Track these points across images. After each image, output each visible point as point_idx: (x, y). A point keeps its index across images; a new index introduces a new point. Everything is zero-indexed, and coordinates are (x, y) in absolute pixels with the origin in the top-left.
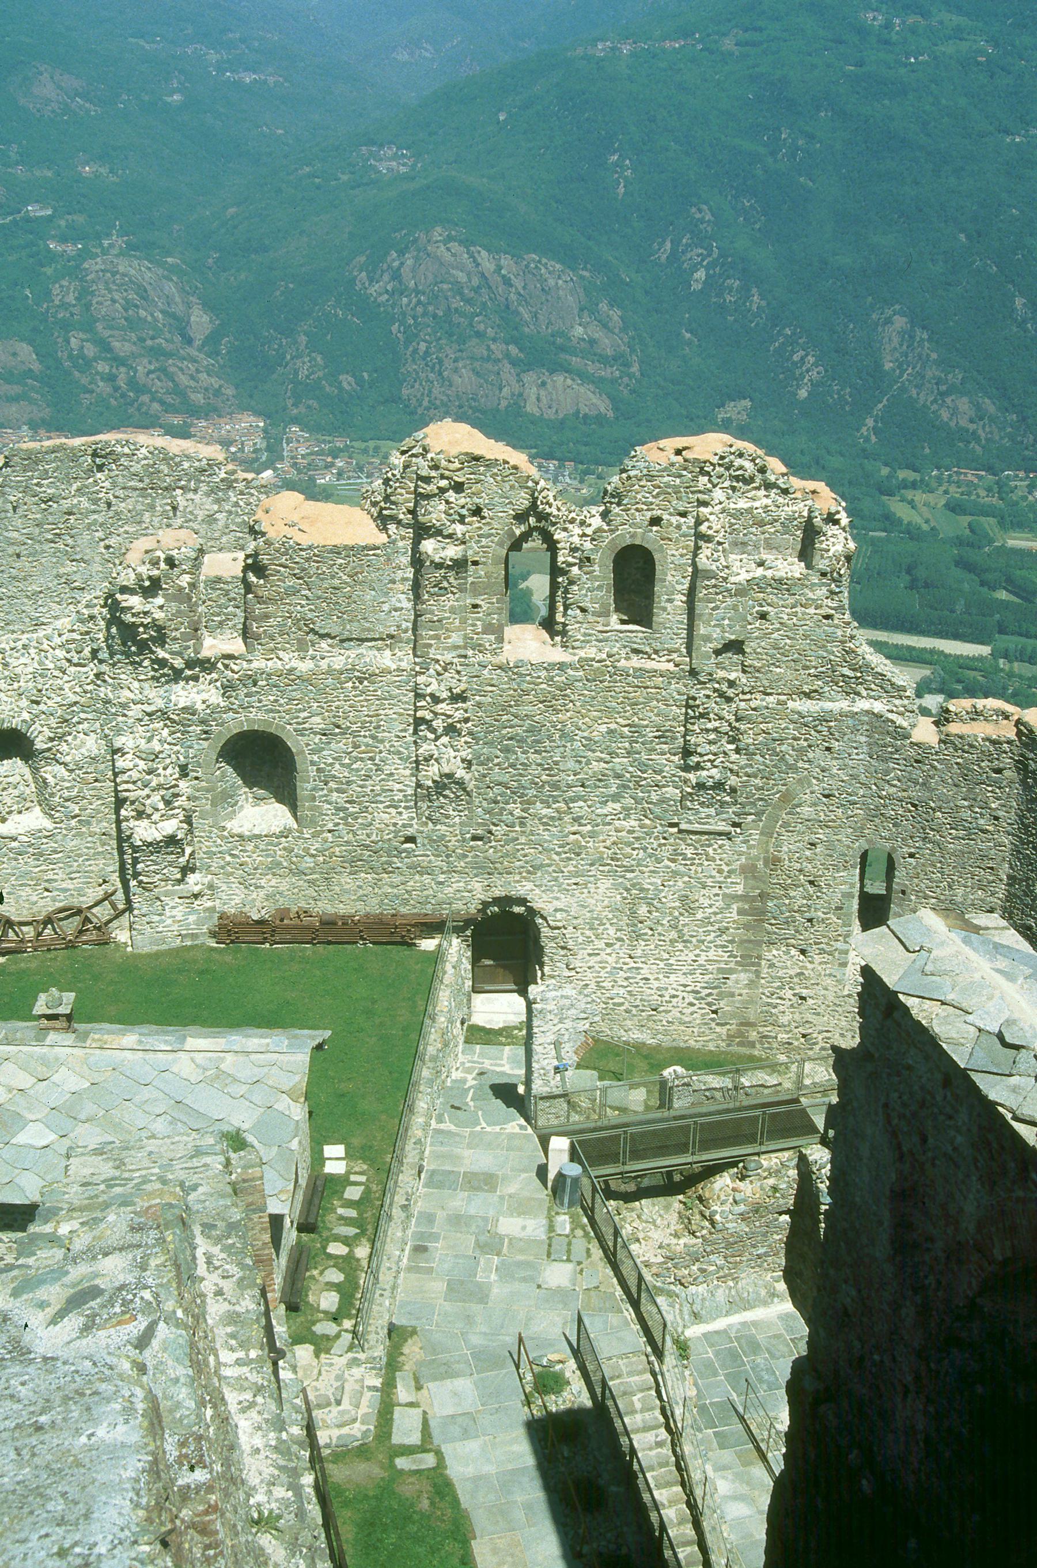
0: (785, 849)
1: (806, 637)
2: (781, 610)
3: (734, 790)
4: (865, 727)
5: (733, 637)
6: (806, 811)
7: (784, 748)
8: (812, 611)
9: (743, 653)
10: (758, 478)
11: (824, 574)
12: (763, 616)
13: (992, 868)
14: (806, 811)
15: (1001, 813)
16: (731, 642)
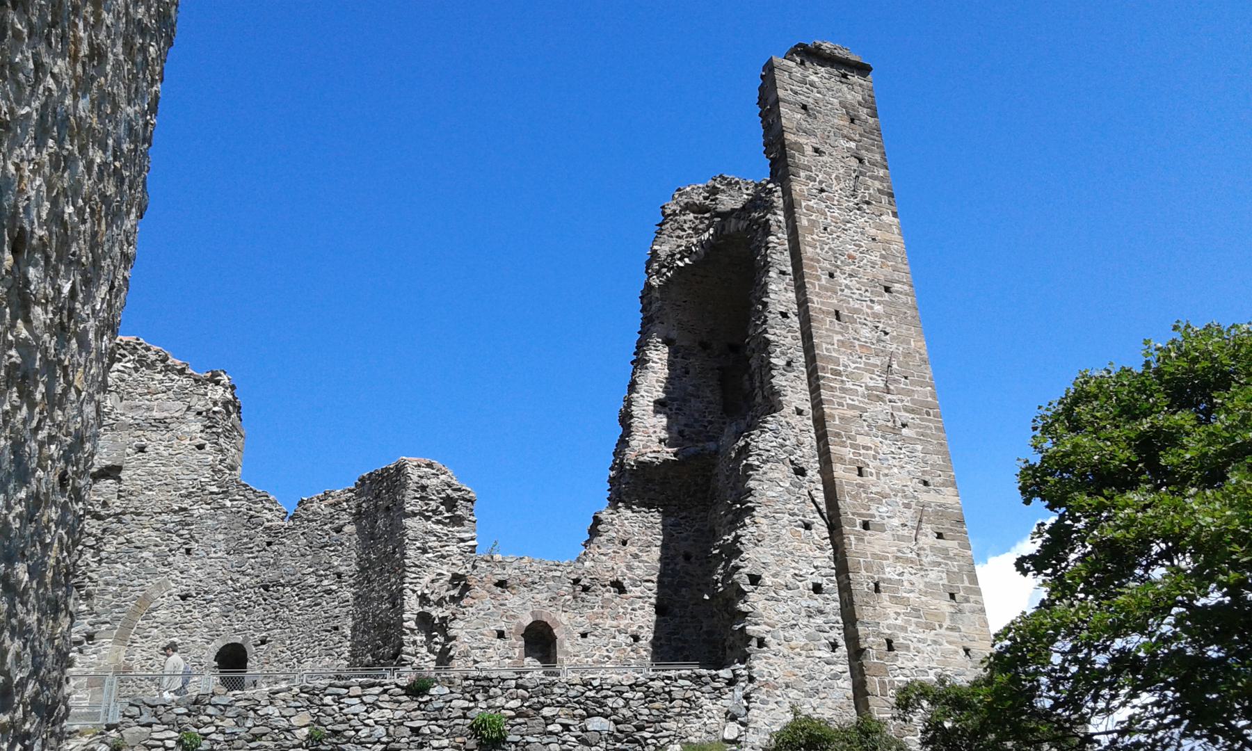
0: (137, 656)
1: (179, 463)
2: (156, 441)
3: (89, 596)
4: (224, 525)
5: (109, 463)
6: (162, 614)
7: (145, 554)
8: (187, 442)
9: (119, 480)
10: (160, 366)
11: (199, 413)
12: (142, 449)
13: (336, 628)
14: (162, 614)
15: (342, 569)
16: (107, 467)
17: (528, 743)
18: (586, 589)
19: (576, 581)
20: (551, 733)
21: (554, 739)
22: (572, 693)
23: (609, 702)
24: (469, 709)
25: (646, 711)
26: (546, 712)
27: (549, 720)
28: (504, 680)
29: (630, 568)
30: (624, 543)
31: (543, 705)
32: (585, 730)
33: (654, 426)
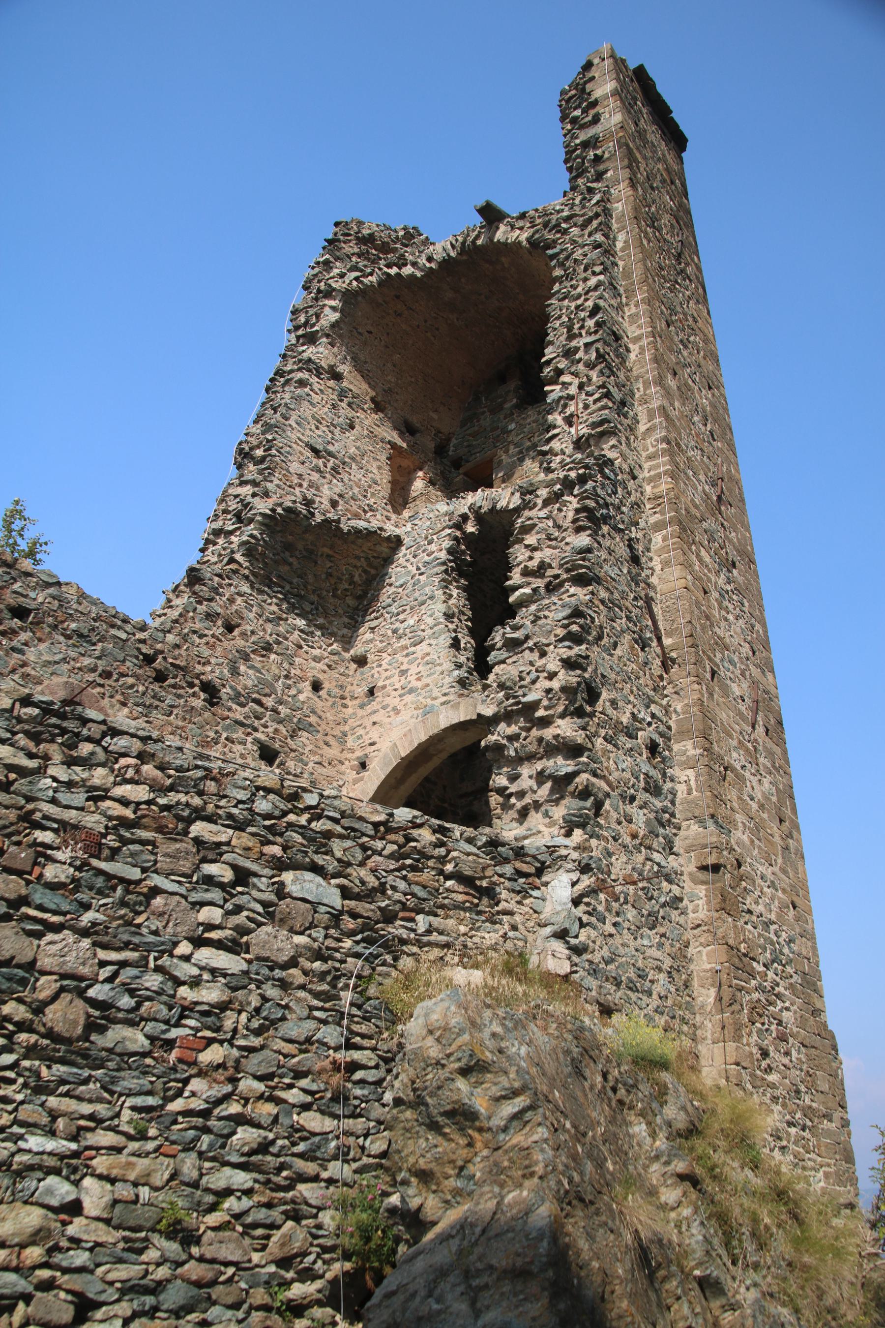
17: (156, 891)
18: (160, 677)
19: (149, 660)
20: (209, 880)
21: (216, 895)
22: (263, 805)
23: (337, 847)
24: (22, 772)
25: (402, 885)
26: (198, 828)
27: (210, 851)
28: (115, 732)
29: (235, 672)
30: (230, 628)
31: (199, 814)
32: (281, 892)
33: (300, 476)
